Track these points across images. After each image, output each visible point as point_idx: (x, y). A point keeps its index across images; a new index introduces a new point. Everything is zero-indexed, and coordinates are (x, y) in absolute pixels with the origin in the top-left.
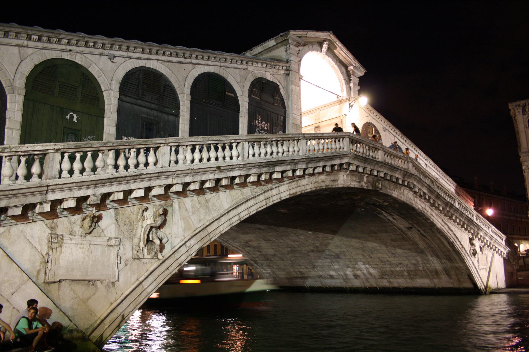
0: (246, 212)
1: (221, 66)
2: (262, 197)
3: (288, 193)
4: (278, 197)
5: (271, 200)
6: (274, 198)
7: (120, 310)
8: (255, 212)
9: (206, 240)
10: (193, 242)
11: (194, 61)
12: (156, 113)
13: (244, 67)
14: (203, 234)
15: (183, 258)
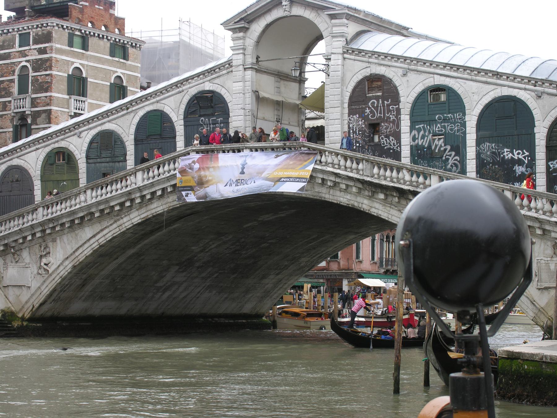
0: (103, 239)
1: (157, 102)
2: (115, 226)
3: (139, 218)
4: (130, 222)
5: (124, 226)
6: (126, 224)
7: (31, 301)
8: (111, 238)
9: (75, 261)
10: (67, 262)
11: (134, 108)
12: (111, 164)
13: (181, 89)
14: (73, 257)
15: (62, 273)
